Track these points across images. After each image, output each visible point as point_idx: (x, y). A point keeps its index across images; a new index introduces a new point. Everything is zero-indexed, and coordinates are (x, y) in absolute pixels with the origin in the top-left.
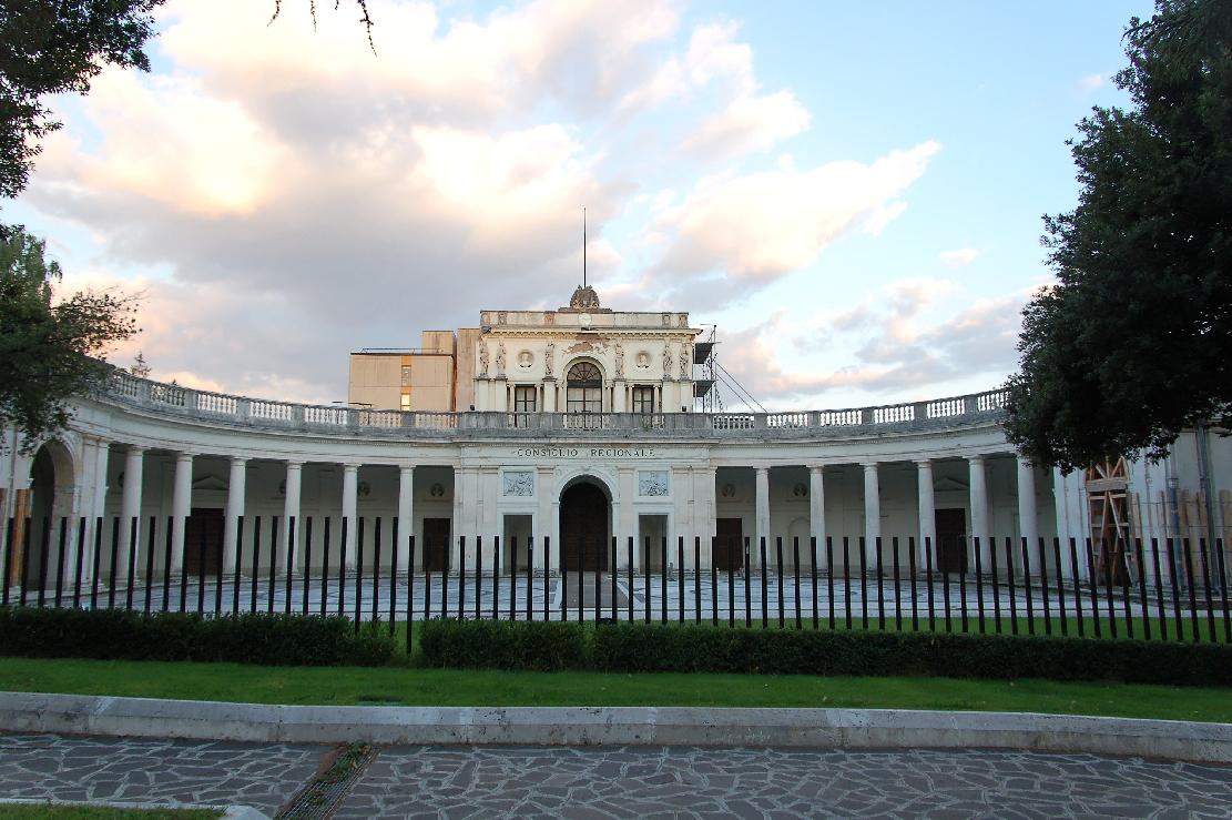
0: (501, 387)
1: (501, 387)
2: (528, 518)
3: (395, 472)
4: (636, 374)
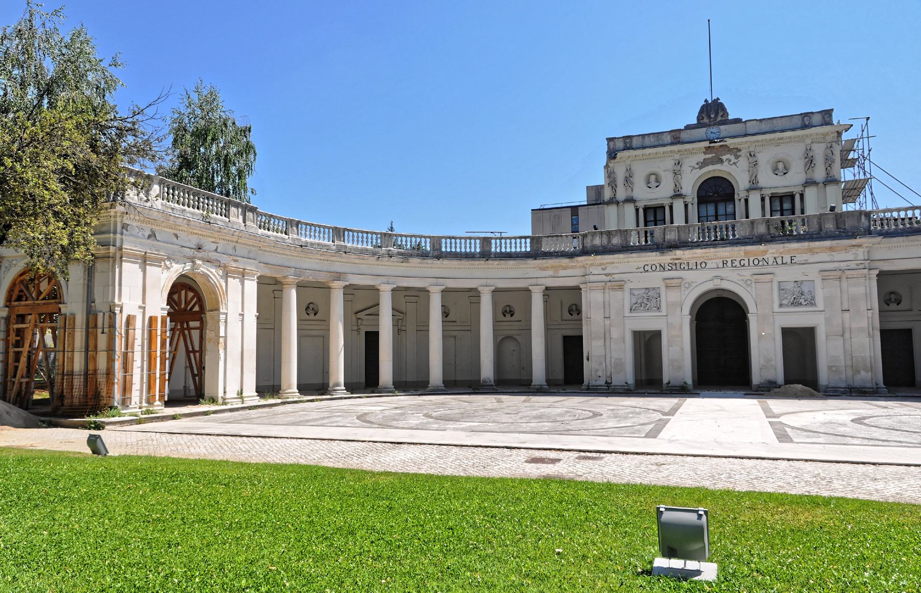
0: (630, 209)
1: (630, 209)
2: (657, 334)
3: (527, 291)
4: (771, 182)
